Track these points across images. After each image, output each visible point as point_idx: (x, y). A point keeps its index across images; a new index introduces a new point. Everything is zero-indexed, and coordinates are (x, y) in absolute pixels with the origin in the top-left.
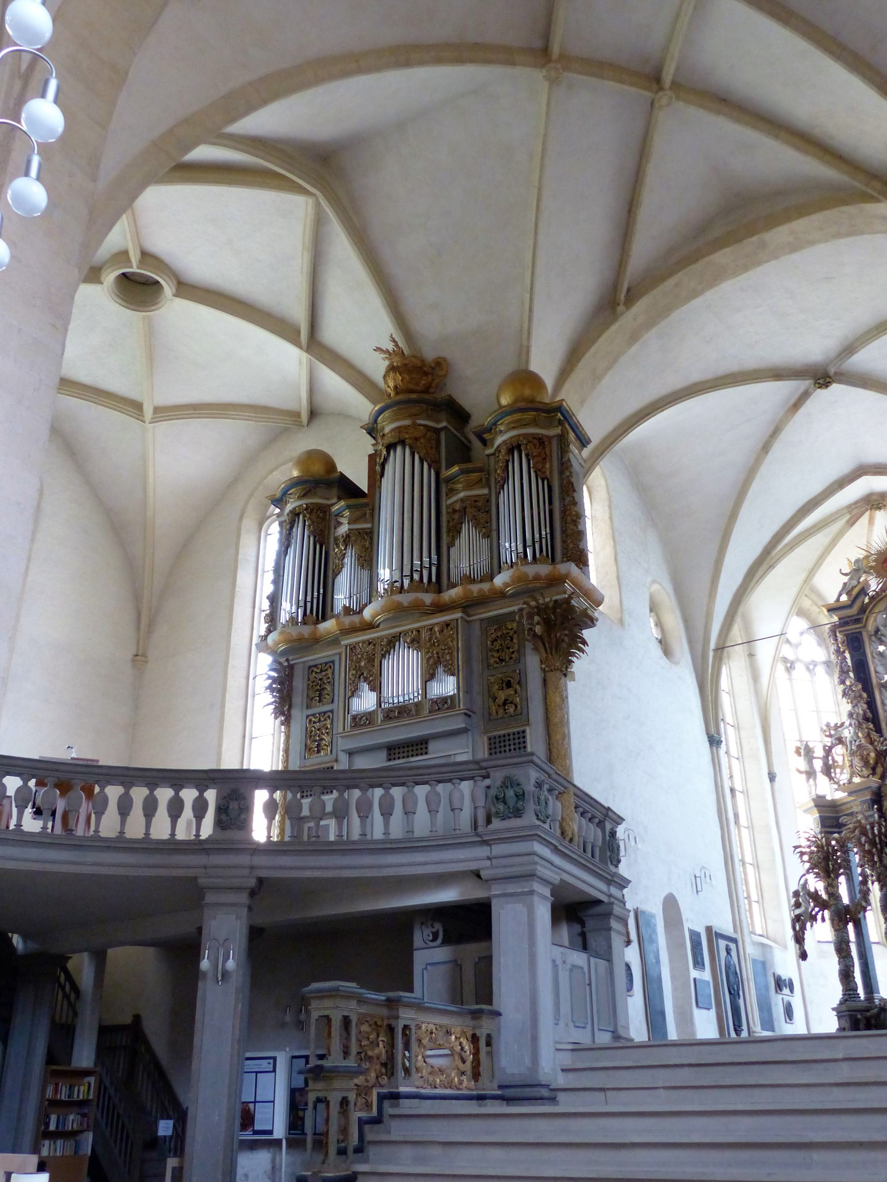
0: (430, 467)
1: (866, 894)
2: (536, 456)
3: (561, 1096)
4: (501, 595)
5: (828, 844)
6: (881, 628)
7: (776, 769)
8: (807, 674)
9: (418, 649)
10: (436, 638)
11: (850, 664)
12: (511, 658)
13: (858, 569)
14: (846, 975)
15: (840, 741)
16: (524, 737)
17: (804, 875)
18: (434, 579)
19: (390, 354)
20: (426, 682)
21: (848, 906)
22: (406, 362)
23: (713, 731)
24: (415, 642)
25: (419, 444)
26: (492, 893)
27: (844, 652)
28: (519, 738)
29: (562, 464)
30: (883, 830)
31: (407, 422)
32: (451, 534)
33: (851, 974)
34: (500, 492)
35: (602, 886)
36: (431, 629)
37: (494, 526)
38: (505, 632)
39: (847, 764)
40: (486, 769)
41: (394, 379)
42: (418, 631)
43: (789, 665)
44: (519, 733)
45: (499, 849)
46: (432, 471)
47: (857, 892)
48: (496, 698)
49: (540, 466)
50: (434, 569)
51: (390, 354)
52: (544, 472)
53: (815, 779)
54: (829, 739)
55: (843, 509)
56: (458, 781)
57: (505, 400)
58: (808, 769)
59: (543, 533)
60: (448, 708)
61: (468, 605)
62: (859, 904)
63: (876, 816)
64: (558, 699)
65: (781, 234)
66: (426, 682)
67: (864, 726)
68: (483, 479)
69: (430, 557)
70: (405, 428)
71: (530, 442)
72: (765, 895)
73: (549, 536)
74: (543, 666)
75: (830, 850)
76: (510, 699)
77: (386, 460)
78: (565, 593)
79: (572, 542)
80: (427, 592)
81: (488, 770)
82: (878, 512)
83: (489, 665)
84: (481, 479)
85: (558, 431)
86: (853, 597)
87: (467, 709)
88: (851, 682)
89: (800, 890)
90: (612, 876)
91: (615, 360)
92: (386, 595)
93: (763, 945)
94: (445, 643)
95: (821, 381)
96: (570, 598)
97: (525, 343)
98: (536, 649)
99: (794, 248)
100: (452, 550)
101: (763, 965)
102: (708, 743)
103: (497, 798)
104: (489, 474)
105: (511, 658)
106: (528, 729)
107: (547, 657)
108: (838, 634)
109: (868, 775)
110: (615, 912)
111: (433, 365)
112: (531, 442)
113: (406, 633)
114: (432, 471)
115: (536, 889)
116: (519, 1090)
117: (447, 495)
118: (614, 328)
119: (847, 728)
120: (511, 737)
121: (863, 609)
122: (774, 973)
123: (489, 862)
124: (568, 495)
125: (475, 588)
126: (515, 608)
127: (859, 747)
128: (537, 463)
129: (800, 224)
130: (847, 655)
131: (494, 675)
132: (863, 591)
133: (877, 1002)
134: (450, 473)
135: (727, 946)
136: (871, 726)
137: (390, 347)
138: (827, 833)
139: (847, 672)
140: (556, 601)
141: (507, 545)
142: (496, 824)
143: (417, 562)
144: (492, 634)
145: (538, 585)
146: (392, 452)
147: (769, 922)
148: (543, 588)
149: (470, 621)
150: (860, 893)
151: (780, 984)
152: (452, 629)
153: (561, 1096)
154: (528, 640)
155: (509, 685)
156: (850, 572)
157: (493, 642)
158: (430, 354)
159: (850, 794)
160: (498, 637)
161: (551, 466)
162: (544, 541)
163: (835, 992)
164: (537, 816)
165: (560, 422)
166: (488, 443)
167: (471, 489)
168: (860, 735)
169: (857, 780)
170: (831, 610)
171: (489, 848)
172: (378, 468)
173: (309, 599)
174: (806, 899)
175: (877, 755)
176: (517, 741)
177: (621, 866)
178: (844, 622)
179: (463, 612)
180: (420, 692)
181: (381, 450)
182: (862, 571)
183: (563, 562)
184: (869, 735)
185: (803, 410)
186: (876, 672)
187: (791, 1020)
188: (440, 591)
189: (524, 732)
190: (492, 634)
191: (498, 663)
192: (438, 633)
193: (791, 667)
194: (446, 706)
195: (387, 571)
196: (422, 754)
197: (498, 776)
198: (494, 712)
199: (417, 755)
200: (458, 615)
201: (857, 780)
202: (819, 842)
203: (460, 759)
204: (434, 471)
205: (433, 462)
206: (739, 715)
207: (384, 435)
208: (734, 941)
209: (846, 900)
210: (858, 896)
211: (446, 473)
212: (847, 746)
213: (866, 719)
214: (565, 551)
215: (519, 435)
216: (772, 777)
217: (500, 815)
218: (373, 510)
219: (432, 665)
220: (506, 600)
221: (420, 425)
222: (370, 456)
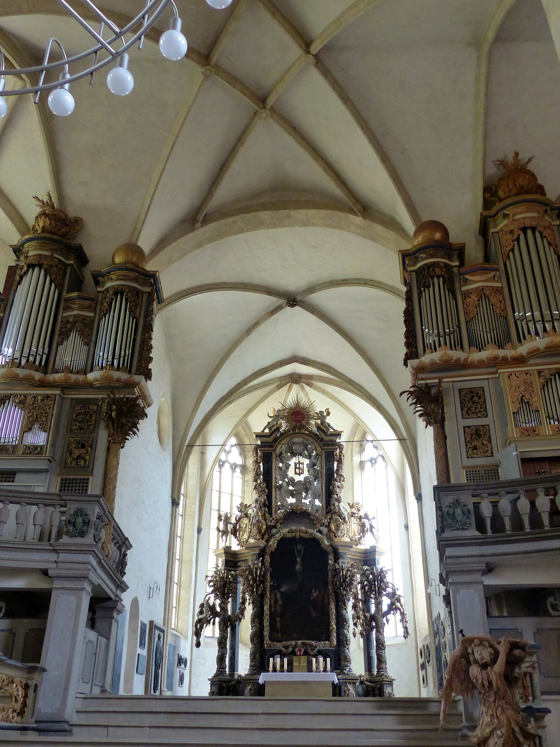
0: (56, 288)
1: (242, 610)
2: (133, 302)
3: (75, 730)
4: (90, 385)
5: (227, 577)
6: (283, 453)
7: (203, 526)
8: (230, 471)
9: (23, 409)
10: (38, 404)
11: (262, 470)
12: (88, 429)
13: (277, 416)
14: (221, 659)
15: (246, 515)
16: (87, 483)
17: (209, 594)
18: (43, 364)
19: (43, 203)
20: (24, 432)
21: (230, 616)
22: (55, 213)
23: (176, 497)
24: (22, 403)
25: (52, 271)
26: (54, 586)
27: (260, 463)
28: (83, 483)
30: (262, 573)
32: (62, 337)
33: (224, 658)
34: (102, 318)
35: (113, 588)
36: (35, 397)
37: (93, 339)
38: (87, 410)
39: (248, 530)
40: (65, 501)
41: (44, 222)
42: (25, 396)
43: (221, 463)
44: (84, 479)
45: (63, 557)
46: (57, 291)
47: (238, 608)
48: (72, 453)
49: (133, 309)
50: (44, 357)
51: (43, 203)
52: (135, 313)
53: (227, 537)
54: (240, 514)
55: (277, 378)
56: (26, 504)
57: (117, 260)
58: (224, 530)
59: (127, 352)
60: (36, 454)
61: (66, 387)
62: (238, 616)
63: (260, 564)
64: (115, 462)
65: (300, 214)
66: (24, 432)
67: (263, 509)
68: (92, 307)
69: (44, 348)
70: (45, 257)
71: (130, 291)
72: (181, 604)
73: (130, 355)
74: (110, 439)
75: (228, 581)
76: (82, 456)
77: (26, 273)
78: (134, 395)
79: (145, 363)
80: (37, 371)
81: (66, 502)
82: (295, 385)
83: (71, 430)
84: (91, 306)
85: (148, 289)
86: (272, 431)
87: (51, 457)
88: (261, 481)
89: (205, 603)
90: (121, 583)
91: (184, 255)
92: (7, 366)
93: (176, 635)
94: (44, 408)
95: (291, 303)
96: (137, 398)
97: (139, 227)
98: (107, 427)
99: (305, 224)
100: (60, 347)
101: (175, 648)
102: (171, 504)
103: (69, 522)
104: (96, 304)
105: (88, 429)
106: (91, 478)
107: (113, 434)
108: (259, 451)
109: (259, 539)
110: (118, 607)
111: (73, 221)
112: (131, 292)
113: (16, 396)
114: (57, 291)
115: (86, 588)
116: (49, 724)
117: (64, 309)
118: (191, 235)
119: (252, 508)
120: (78, 481)
121: (275, 440)
122: (178, 654)
123: (55, 565)
124: (148, 332)
125: (73, 377)
126: (100, 397)
127: (258, 521)
128: (132, 306)
129: (312, 212)
130: (261, 465)
131: (73, 438)
132: (278, 429)
133: (236, 677)
134: (69, 296)
135: (159, 634)
136: (267, 510)
137: (46, 199)
138: (228, 570)
139: (259, 475)
140: (127, 398)
141: (101, 354)
142: (65, 539)
143: (34, 349)
144: (78, 410)
145: (118, 385)
146: (31, 270)
147: (180, 621)
148: (118, 388)
149: (65, 398)
150: (239, 609)
151: (181, 661)
152: (51, 401)
153: (75, 730)
154: (103, 419)
155: (83, 446)
156: (274, 416)
157: (77, 415)
158: (72, 213)
159: (246, 548)
160: (81, 412)
161: (140, 310)
162: (126, 357)
163: (212, 669)
164: (94, 538)
165: (151, 285)
166: (100, 284)
167: (82, 311)
168: (260, 514)
169: (252, 541)
170: (258, 436)
171: (56, 555)
172: (17, 277)
174: (207, 609)
175: (266, 528)
176: (81, 485)
177: (125, 577)
178: (263, 445)
179: (62, 391)
180: (18, 438)
181: (23, 266)
182: (280, 418)
183: (136, 374)
184: (264, 514)
185: (275, 316)
186: (276, 478)
187: (182, 685)
188: (46, 373)
189: (88, 479)
190: (78, 410)
191: (78, 430)
192: (40, 401)
193: (222, 465)
194: (36, 452)
195: (11, 350)
196: (9, 481)
197: (72, 507)
198: (69, 462)
199: (5, 481)
200: (58, 392)
201: (252, 541)
202: (221, 575)
203: (37, 490)
204: (58, 291)
205: (59, 285)
206: (188, 488)
207: (27, 257)
208: (163, 631)
209: (229, 613)
210: (238, 611)
211: (65, 295)
212: (250, 519)
213: (265, 505)
214: (139, 367)
215: (124, 285)
216: (199, 531)
217: (69, 534)
218: (6, 305)
219: (31, 422)
220: (92, 390)
221: (55, 258)
222: (10, 267)
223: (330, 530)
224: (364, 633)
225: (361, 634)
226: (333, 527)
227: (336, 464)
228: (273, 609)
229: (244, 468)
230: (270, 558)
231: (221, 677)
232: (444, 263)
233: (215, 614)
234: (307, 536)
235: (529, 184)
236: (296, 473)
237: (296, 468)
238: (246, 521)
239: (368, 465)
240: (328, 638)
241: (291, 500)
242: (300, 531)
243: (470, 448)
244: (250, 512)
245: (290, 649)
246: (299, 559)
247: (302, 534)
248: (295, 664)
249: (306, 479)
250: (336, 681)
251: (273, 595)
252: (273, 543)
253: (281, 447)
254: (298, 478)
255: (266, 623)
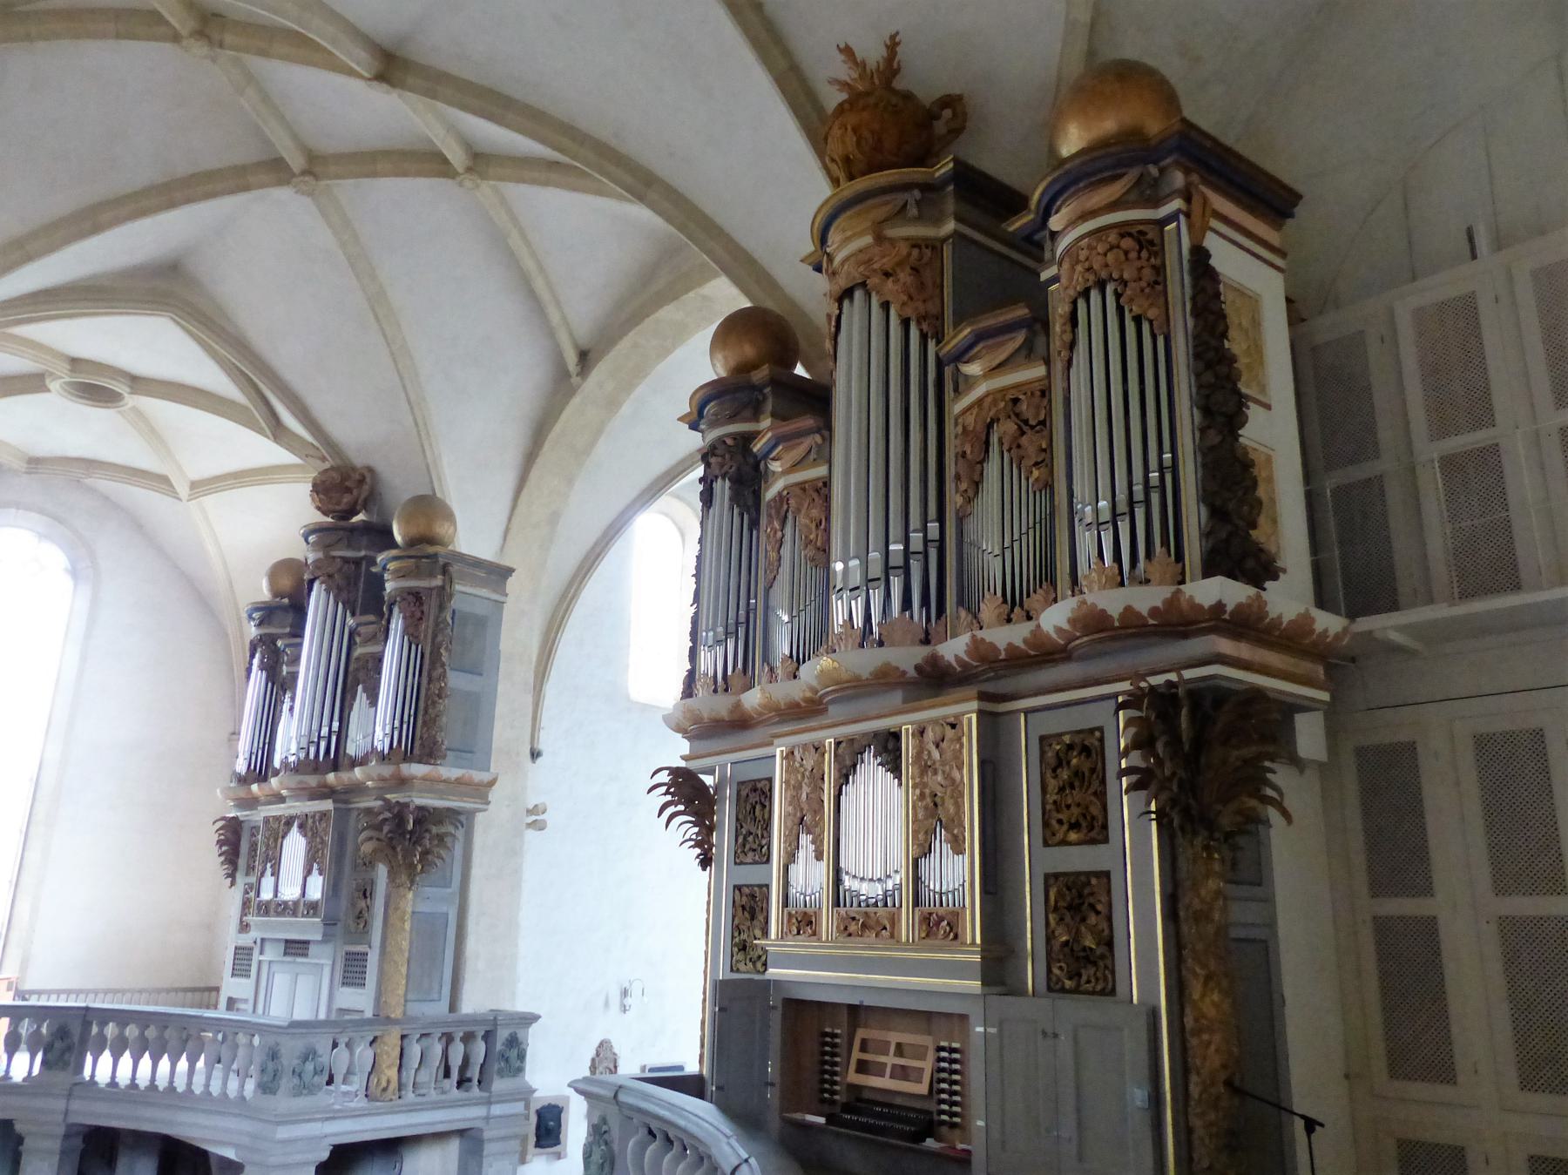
29: (437, 624)
50: (334, 738)
158: (359, 461)
173: (261, 745)
221: (334, 557)
232: (734, 436)
235: (858, 143)
243: (736, 945)
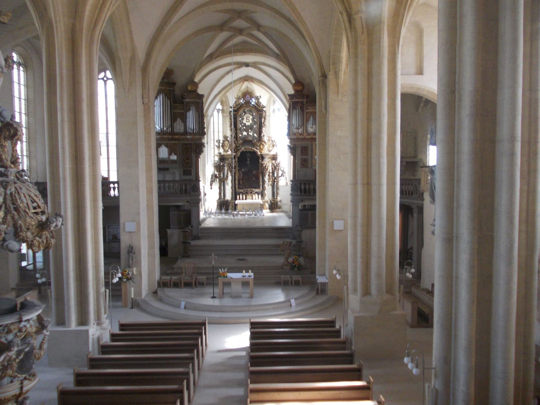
0: (169, 100)
1: (227, 177)
14: (220, 194)
15: (227, 140)
24: (167, 146)
31: (164, 88)
62: (226, 179)
136: (236, 139)
155: (188, 159)
163: (217, 197)
223: (260, 148)
224: (272, 184)
225: (271, 185)
226: (261, 147)
227: (263, 119)
228: (239, 178)
229: (223, 111)
230: (238, 159)
231: (221, 200)
233: (217, 177)
234: (252, 151)
236: (247, 121)
237: (247, 119)
238: (226, 142)
239: (276, 111)
240: (259, 188)
241: (245, 133)
242: (249, 148)
244: (229, 139)
245: (246, 192)
246: (248, 159)
247: (250, 150)
248: (248, 197)
249: (251, 124)
250: (262, 203)
251: (239, 173)
252: (239, 154)
253: (241, 111)
254: (248, 124)
255: (237, 183)
